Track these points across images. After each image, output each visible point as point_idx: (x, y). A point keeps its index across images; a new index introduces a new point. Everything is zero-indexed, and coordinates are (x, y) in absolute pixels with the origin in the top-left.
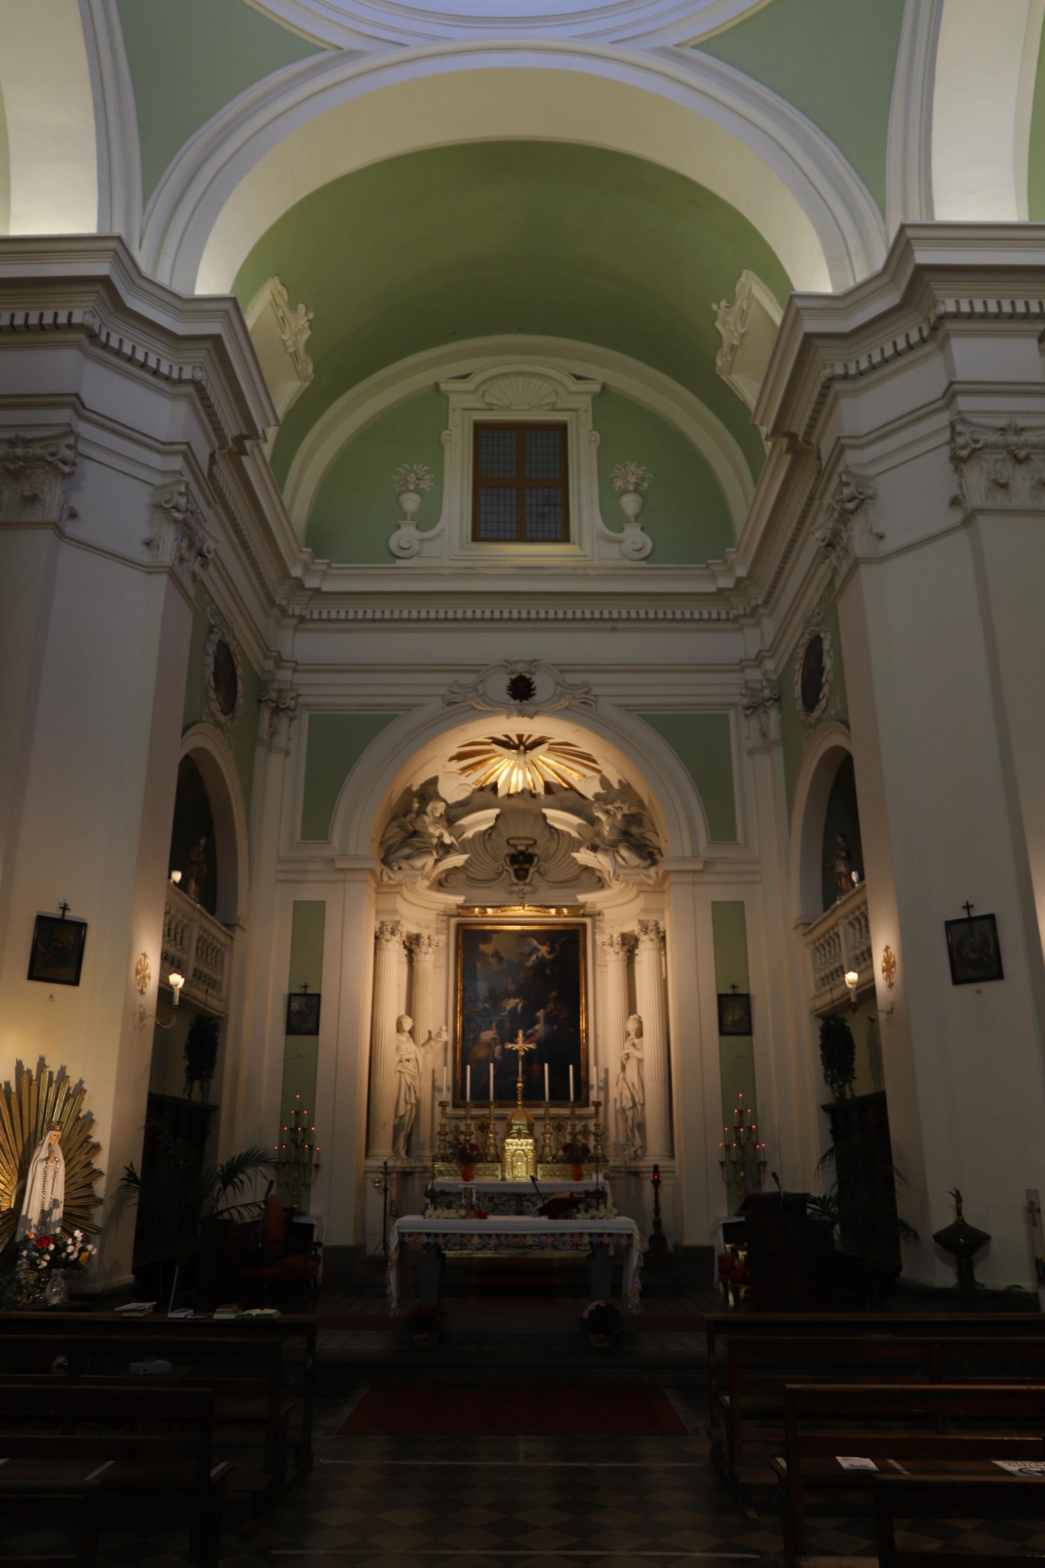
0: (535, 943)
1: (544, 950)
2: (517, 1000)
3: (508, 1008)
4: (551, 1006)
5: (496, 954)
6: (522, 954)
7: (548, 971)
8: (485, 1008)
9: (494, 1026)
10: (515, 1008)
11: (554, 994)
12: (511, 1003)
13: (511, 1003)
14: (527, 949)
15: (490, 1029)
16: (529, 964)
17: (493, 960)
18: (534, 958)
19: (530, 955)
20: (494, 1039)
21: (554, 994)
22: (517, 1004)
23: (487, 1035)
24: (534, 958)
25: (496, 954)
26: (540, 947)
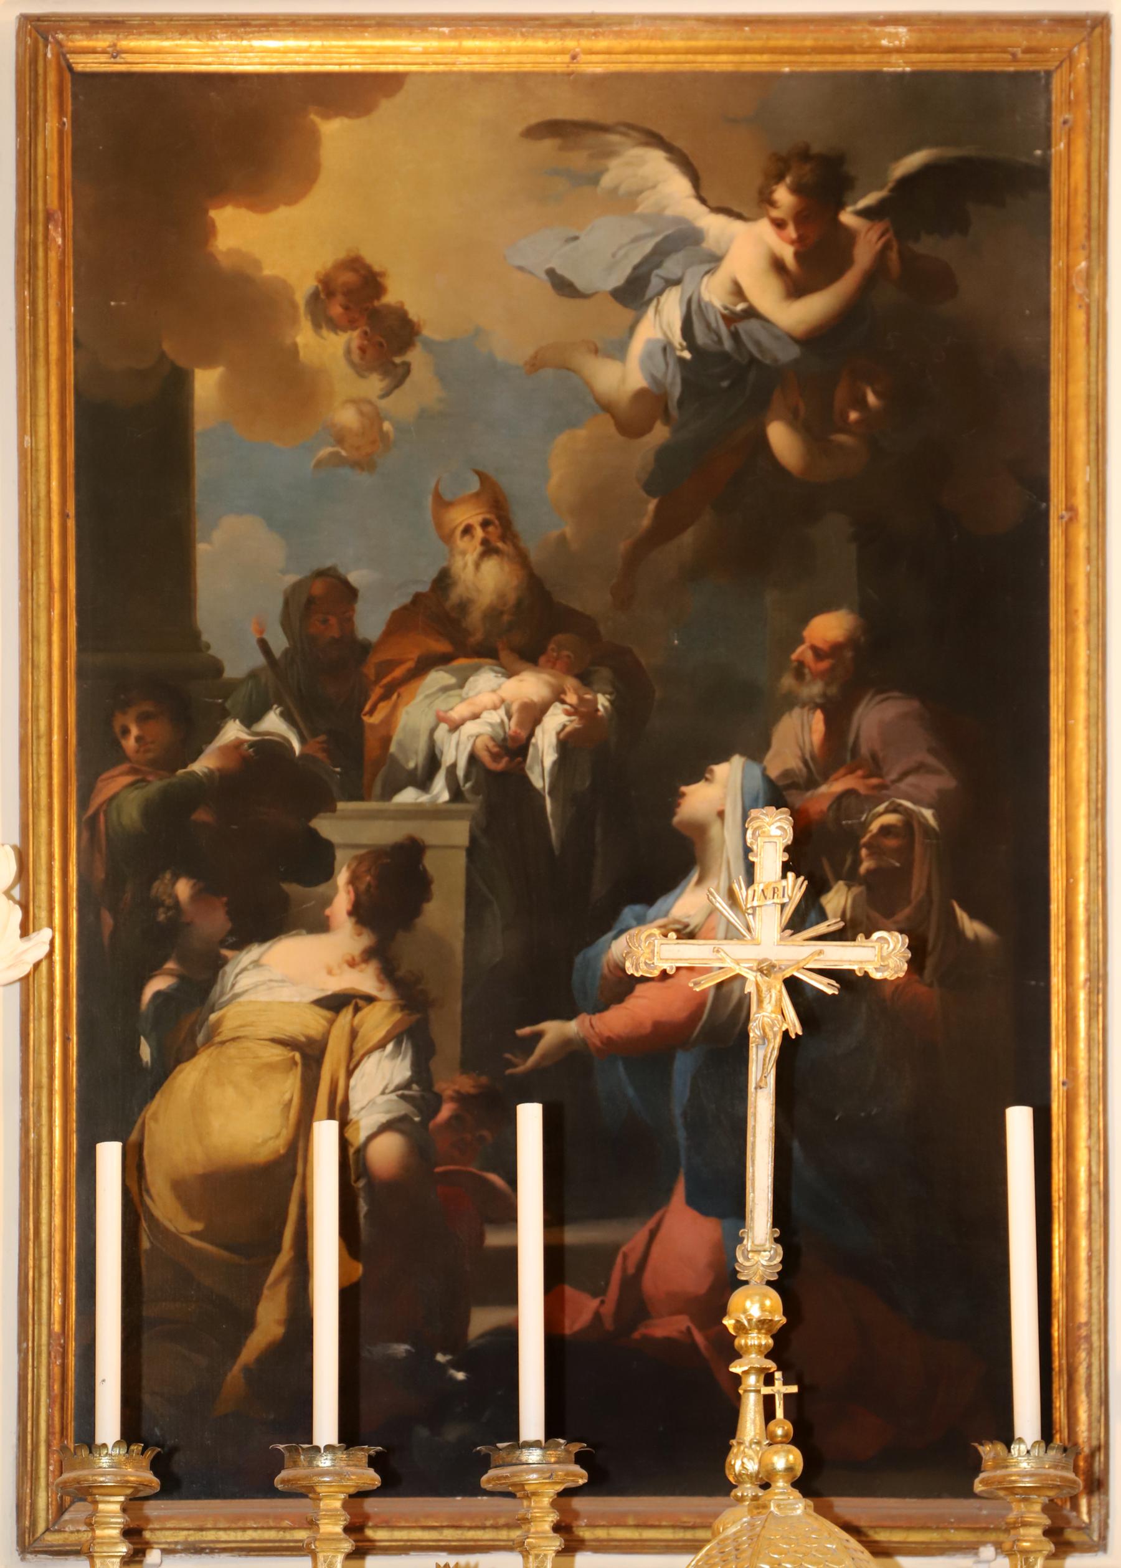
0: (673, 191)
1: (747, 253)
2: (530, 685)
3: (455, 751)
4: (799, 733)
5: (355, 295)
6: (563, 286)
7: (781, 438)
8: (269, 751)
9: (342, 902)
10: (515, 749)
11: (829, 627)
12: (469, 710)
13: (469, 710)
14: (603, 253)
15: (320, 925)
16: (624, 376)
17: (326, 349)
18: (663, 321)
19: (635, 293)
20: (335, 1003)
21: (829, 627)
22: (534, 714)
23: (286, 978)
24: (663, 321)
25: (355, 295)
26: (713, 225)
